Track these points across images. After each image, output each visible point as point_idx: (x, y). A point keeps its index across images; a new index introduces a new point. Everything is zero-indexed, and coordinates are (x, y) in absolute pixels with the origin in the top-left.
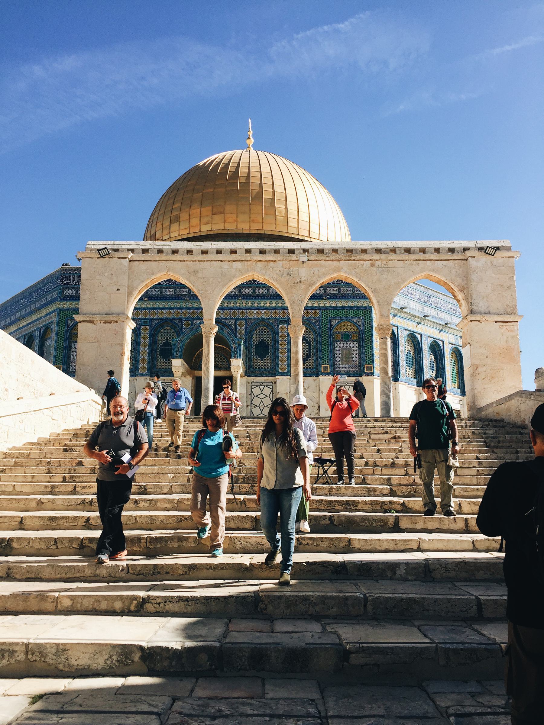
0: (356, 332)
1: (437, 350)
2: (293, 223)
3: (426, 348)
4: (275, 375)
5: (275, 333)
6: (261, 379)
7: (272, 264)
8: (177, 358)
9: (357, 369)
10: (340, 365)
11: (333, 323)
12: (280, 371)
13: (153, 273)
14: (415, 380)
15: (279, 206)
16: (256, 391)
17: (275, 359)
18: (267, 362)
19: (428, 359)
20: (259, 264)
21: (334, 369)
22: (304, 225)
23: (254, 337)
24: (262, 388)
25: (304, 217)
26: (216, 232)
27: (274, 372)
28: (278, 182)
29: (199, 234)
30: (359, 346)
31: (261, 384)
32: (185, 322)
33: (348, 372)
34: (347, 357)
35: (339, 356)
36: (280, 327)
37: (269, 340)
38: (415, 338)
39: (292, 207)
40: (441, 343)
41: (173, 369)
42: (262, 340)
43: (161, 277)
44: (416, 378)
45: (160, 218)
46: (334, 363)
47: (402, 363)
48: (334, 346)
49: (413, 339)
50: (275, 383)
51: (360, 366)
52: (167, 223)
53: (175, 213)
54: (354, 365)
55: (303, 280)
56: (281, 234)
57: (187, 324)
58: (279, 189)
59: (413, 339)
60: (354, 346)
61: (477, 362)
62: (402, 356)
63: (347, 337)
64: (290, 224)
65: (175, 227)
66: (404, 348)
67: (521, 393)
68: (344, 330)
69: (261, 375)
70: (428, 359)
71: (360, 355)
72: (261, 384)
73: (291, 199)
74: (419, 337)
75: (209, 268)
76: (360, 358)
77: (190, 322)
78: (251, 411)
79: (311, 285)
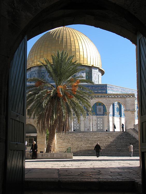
2: (82, 59)
10: (98, 113)
15: (77, 54)
22: (85, 59)
25: (85, 56)
28: (77, 44)
34: (100, 109)
35: (98, 110)
39: (81, 53)
45: (36, 55)
47: (116, 111)
52: (38, 57)
53: (42, 54)
54: (102, 113)
58: (77, 47)
61: (127, 120)
62: (115, 109)
64: (81, 59)
67: (131, 129)
71: (103, 110)
73: (81, 50)
76: (103, 110)
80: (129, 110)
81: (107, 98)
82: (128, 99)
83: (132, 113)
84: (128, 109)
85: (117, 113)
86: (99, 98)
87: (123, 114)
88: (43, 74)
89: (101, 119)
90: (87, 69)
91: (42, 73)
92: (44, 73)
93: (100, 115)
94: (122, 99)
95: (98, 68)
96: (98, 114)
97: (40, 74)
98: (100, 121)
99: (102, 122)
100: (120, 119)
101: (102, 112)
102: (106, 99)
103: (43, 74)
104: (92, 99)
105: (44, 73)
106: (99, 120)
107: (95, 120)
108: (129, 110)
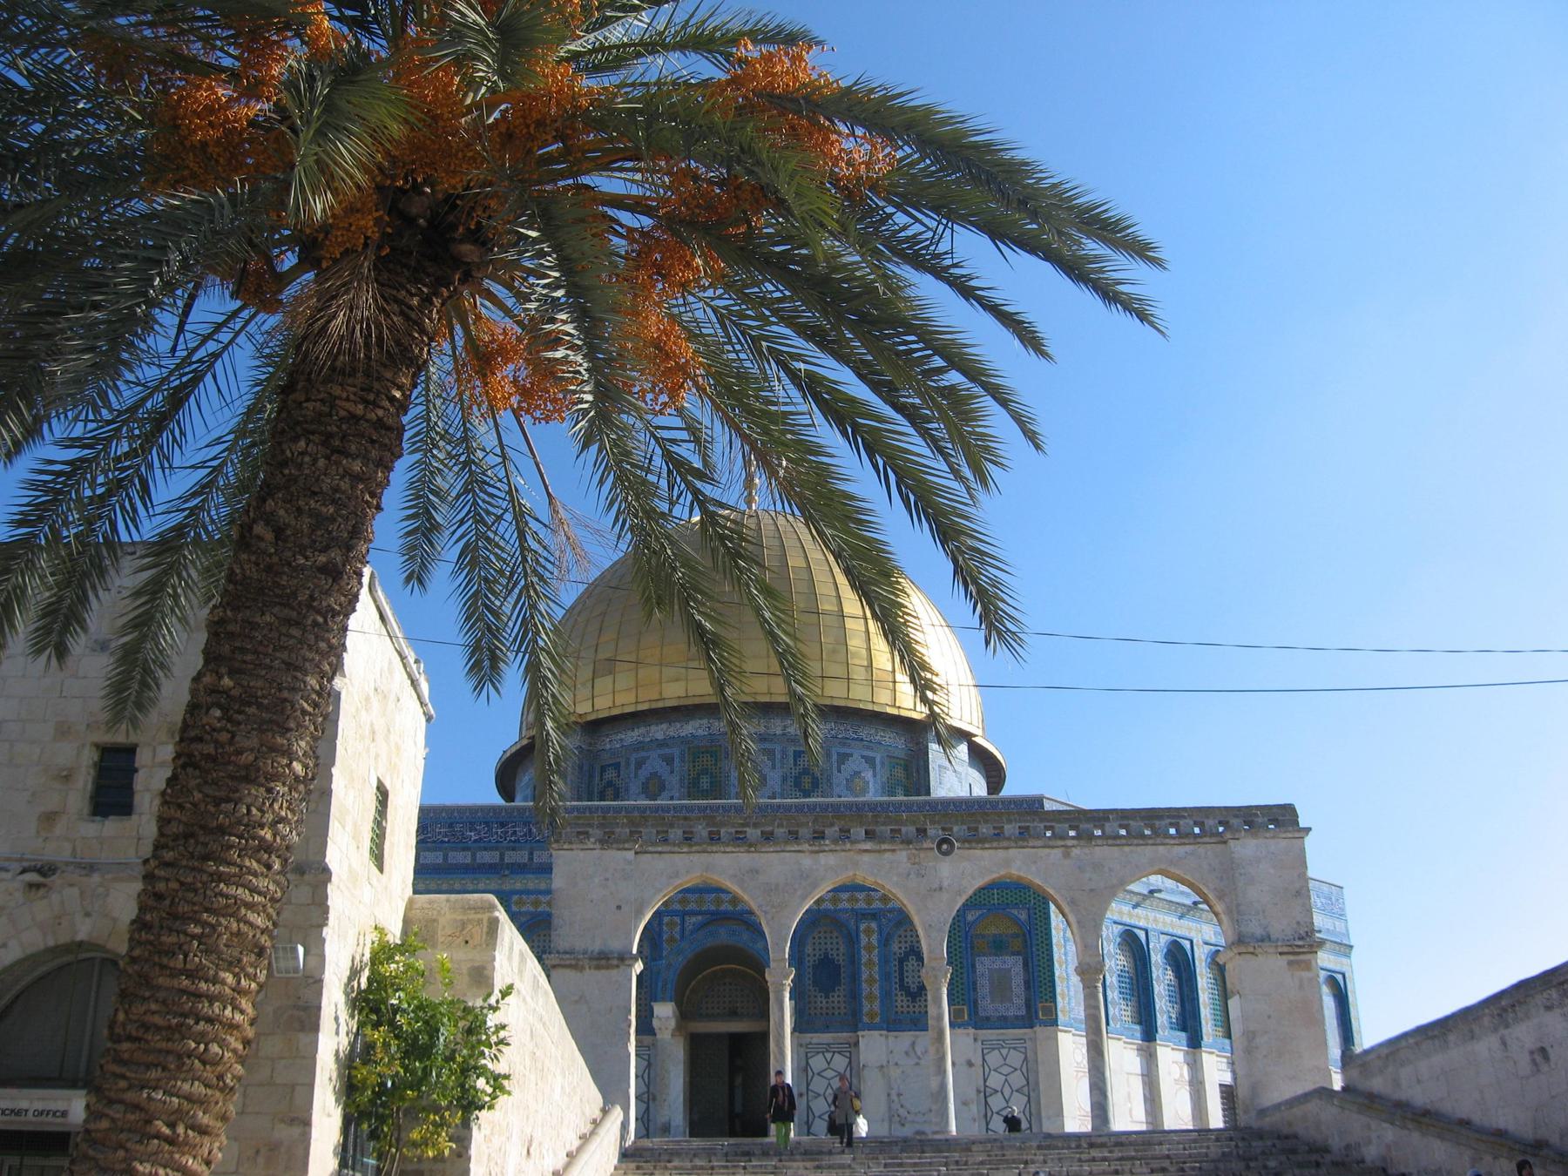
0: (1017, 936)
1: (1180, 959)
3: (1157, 958)
4: (854, 1028)
5: (852, 940)
6: (826, 1037)
7: (887, 855)
8: (664, 1000)
9: (1023, 1012)
10: (987, 1006)
11: (970, 918)
12: (866, 1019)
13: (677, 875)
14: (1138, 1027)
16: (817, 1062)
17: (854, 996)
18: (838, 997)
19: (1162, 980)
20: (866, 858)
21: (976, 1013)
23: (809, 949)
24: (828, 1056)
26: (697, 701)
27: (853, 1022)
29: (660, 705)
30: (1026, 964)
31: (828, 1048)
32: (666, 919)
33: (1005, 1018)
34: (1001, 986)
35: (984, 987)
36: (862, 927)
37: (839, 953)
38: (1135, 938)
40: (1187, 945)
41: (655, 1023)
42: (826, 955)
43: (689, 879)
44: (1140, 1023)
46: (976, 1002)
48: (973, 966)
49: (1133, 944)
50: (857, 1044)
51: (1028, 1006)
52: (585, 673)
54: (1016, 1007)
55: (945, 884)
56: (836, 703)
57: (671, 924)
59: (1133, 944)
60: (1014, 965)
63: (999, 947)
65: (604, 683)
66: (1115, 962)
68: (993, 930)
69: (826, 1029)
70: (1162, 980)
71: (1027, 983)
72: (828, 1048)
74: (1142, 935)
75: (777, 864)
77: (677, 920)
78: (809, 1107)
79: (959, 893)
80: (1266, 938)
81: (1070, 843)
82: (1246, 847)
83: (1290, 963)
84: (1259, 932)
85: (1120, 1010)
86: (1005, 844)
87: (1162, 1020)
88: (610, 774)
89: (1016, 1058)
90: (895, 742)
91: (603, 769)
92: (617, 766)
93: (1004, 1022)
94: (1201, 850)
95: (965, 736)
96: (988, 1018)
97: (591, 776)
98: (1005, 1070)
99: (1017, 1080)
100: (1149, 1060)
101: (1019, 1000)
102: (1067, 855)
103: (610, 774)
104: (946, 854)
105: (617, 766)
106: (994, 1058)
107: (970, 1064)
108: (1266, 938)
